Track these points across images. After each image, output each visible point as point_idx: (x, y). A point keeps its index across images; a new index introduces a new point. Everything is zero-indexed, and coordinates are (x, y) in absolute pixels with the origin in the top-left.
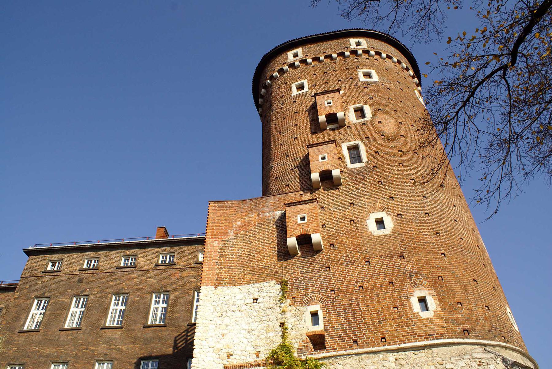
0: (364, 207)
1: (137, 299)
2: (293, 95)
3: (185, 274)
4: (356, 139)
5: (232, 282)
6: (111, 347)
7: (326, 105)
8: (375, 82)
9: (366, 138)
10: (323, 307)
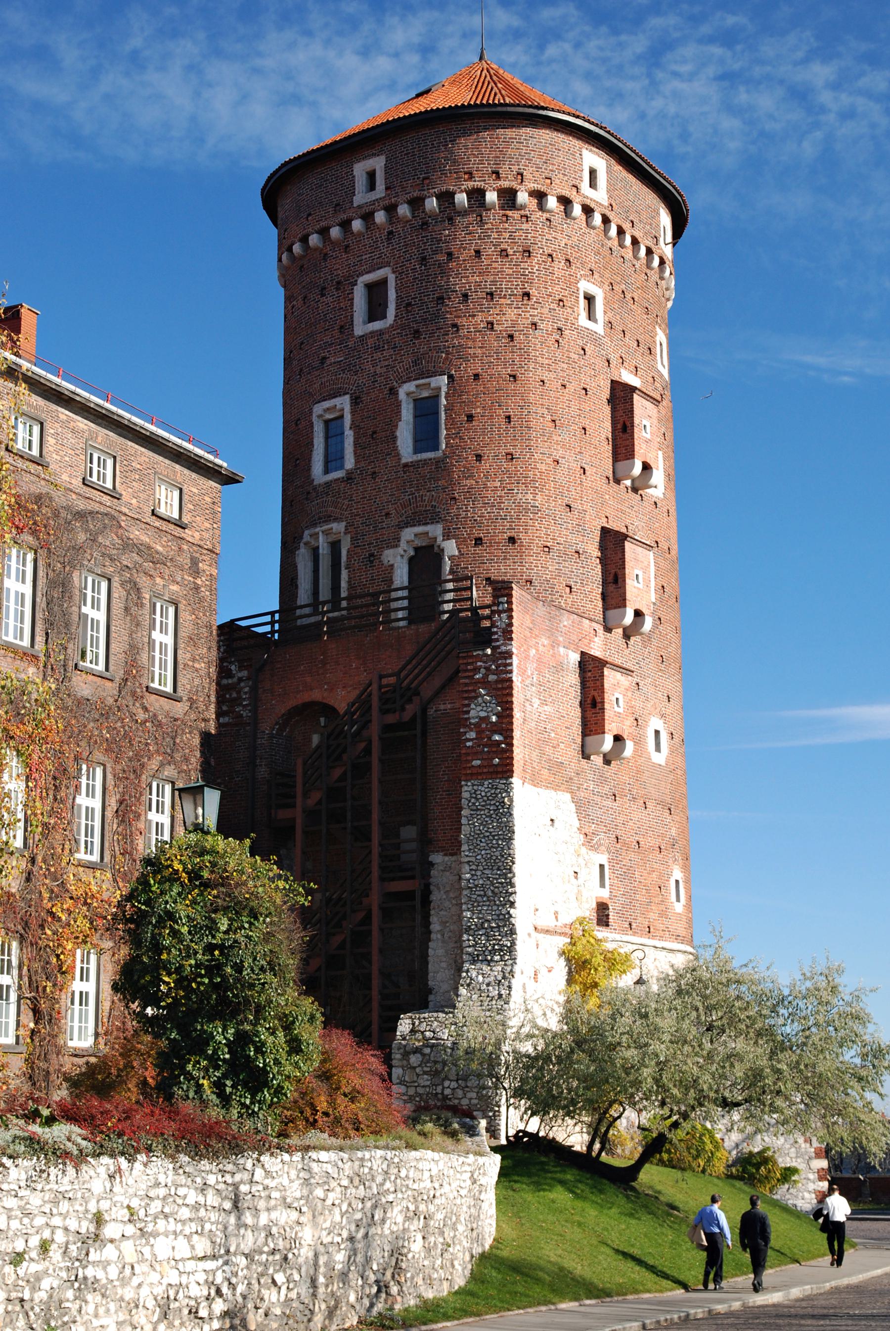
5: (535, 781)
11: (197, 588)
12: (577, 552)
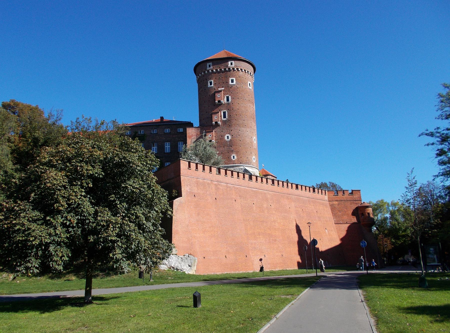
8: (234, 85)
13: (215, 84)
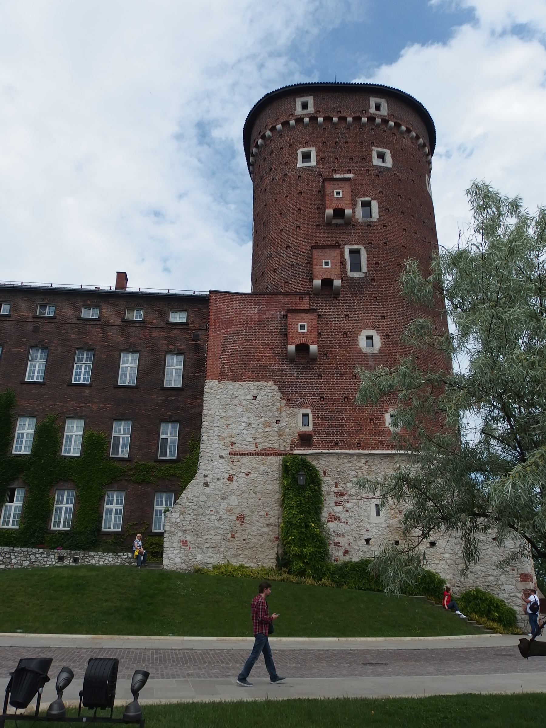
0: (358, 322)
1: (104, 356)
2: (298, 166)
3: (155, 334)
4: (360, 244)
5: (235, 378)
6: (81, 405)
7: (335, 196)
8: (387, 169)
9: (369, 243)
10: (313, 412)
11: (199, 344)
12: (293, 265)
13: (320, 160)
